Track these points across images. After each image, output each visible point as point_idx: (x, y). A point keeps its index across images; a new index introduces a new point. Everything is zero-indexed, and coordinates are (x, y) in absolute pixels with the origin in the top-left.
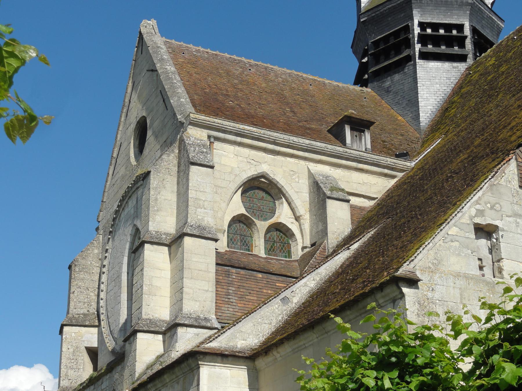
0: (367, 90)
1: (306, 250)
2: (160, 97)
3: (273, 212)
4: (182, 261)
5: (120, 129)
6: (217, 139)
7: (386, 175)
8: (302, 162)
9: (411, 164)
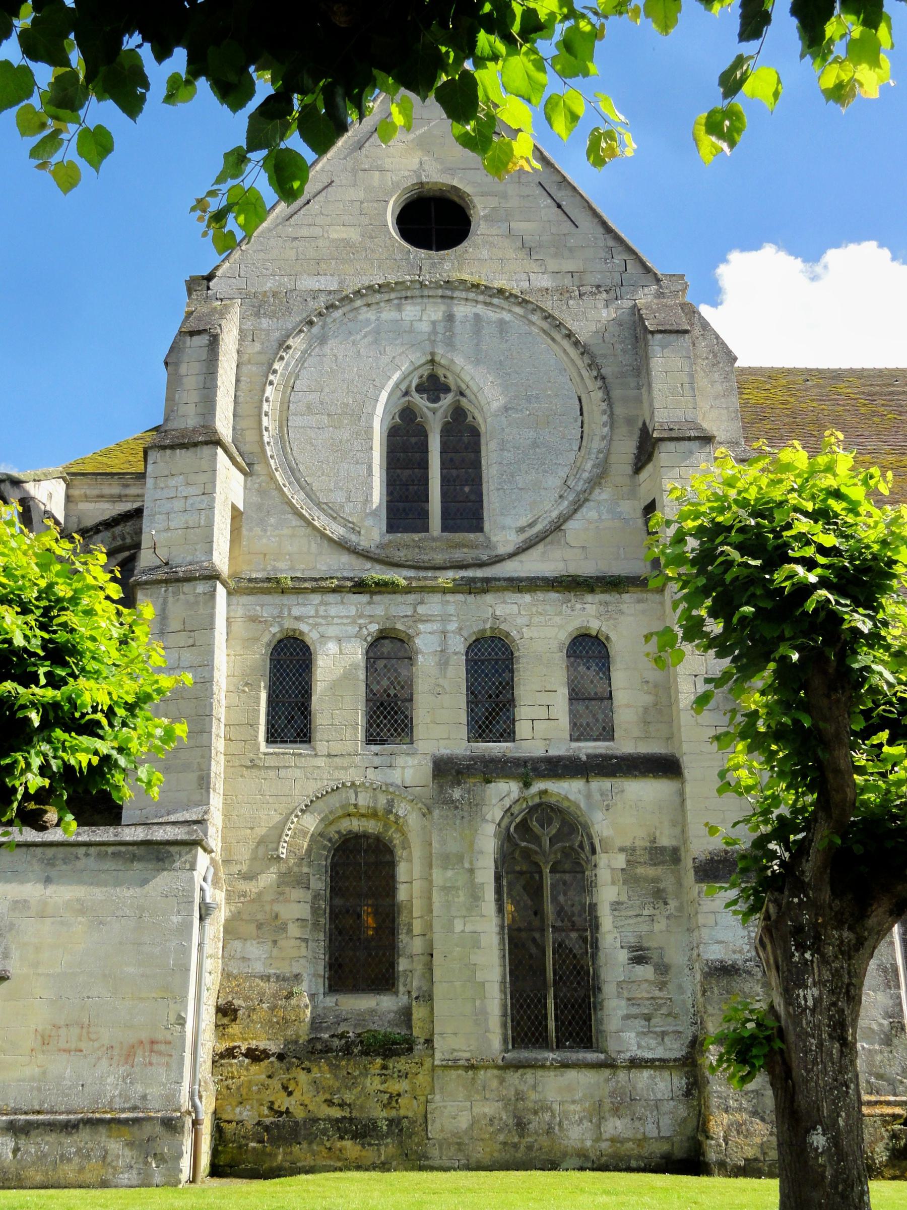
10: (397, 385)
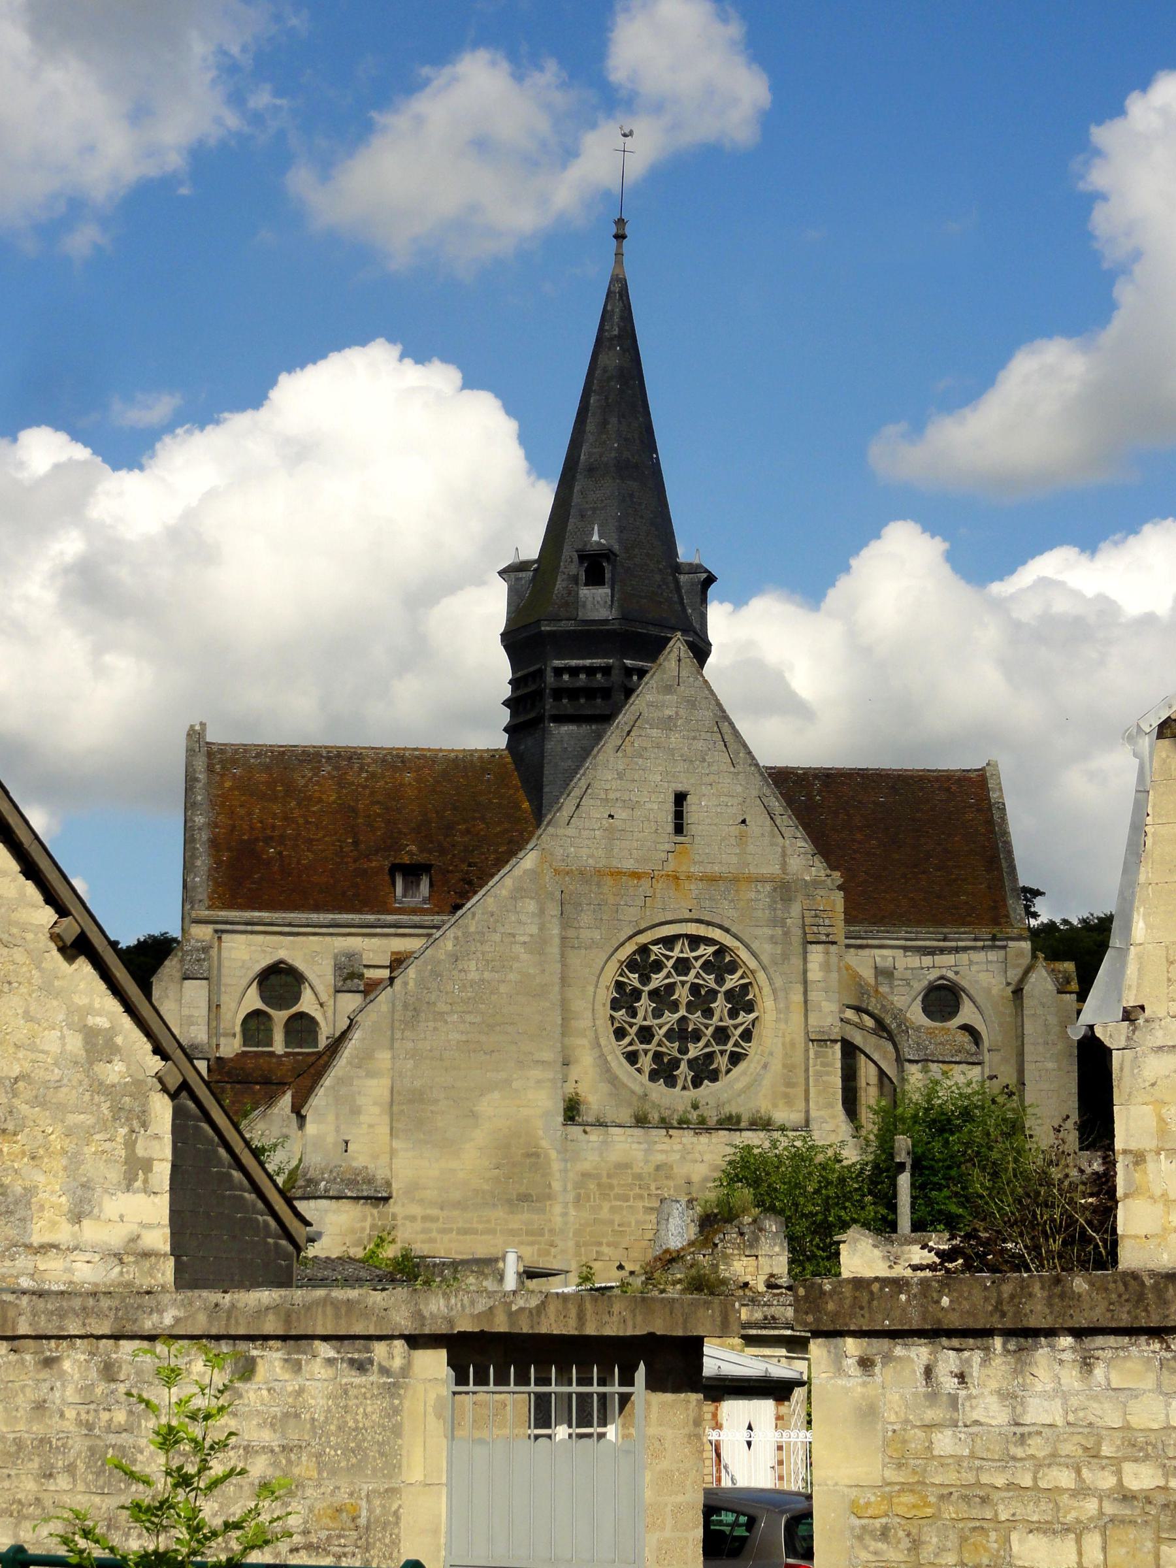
3: (297, 998)
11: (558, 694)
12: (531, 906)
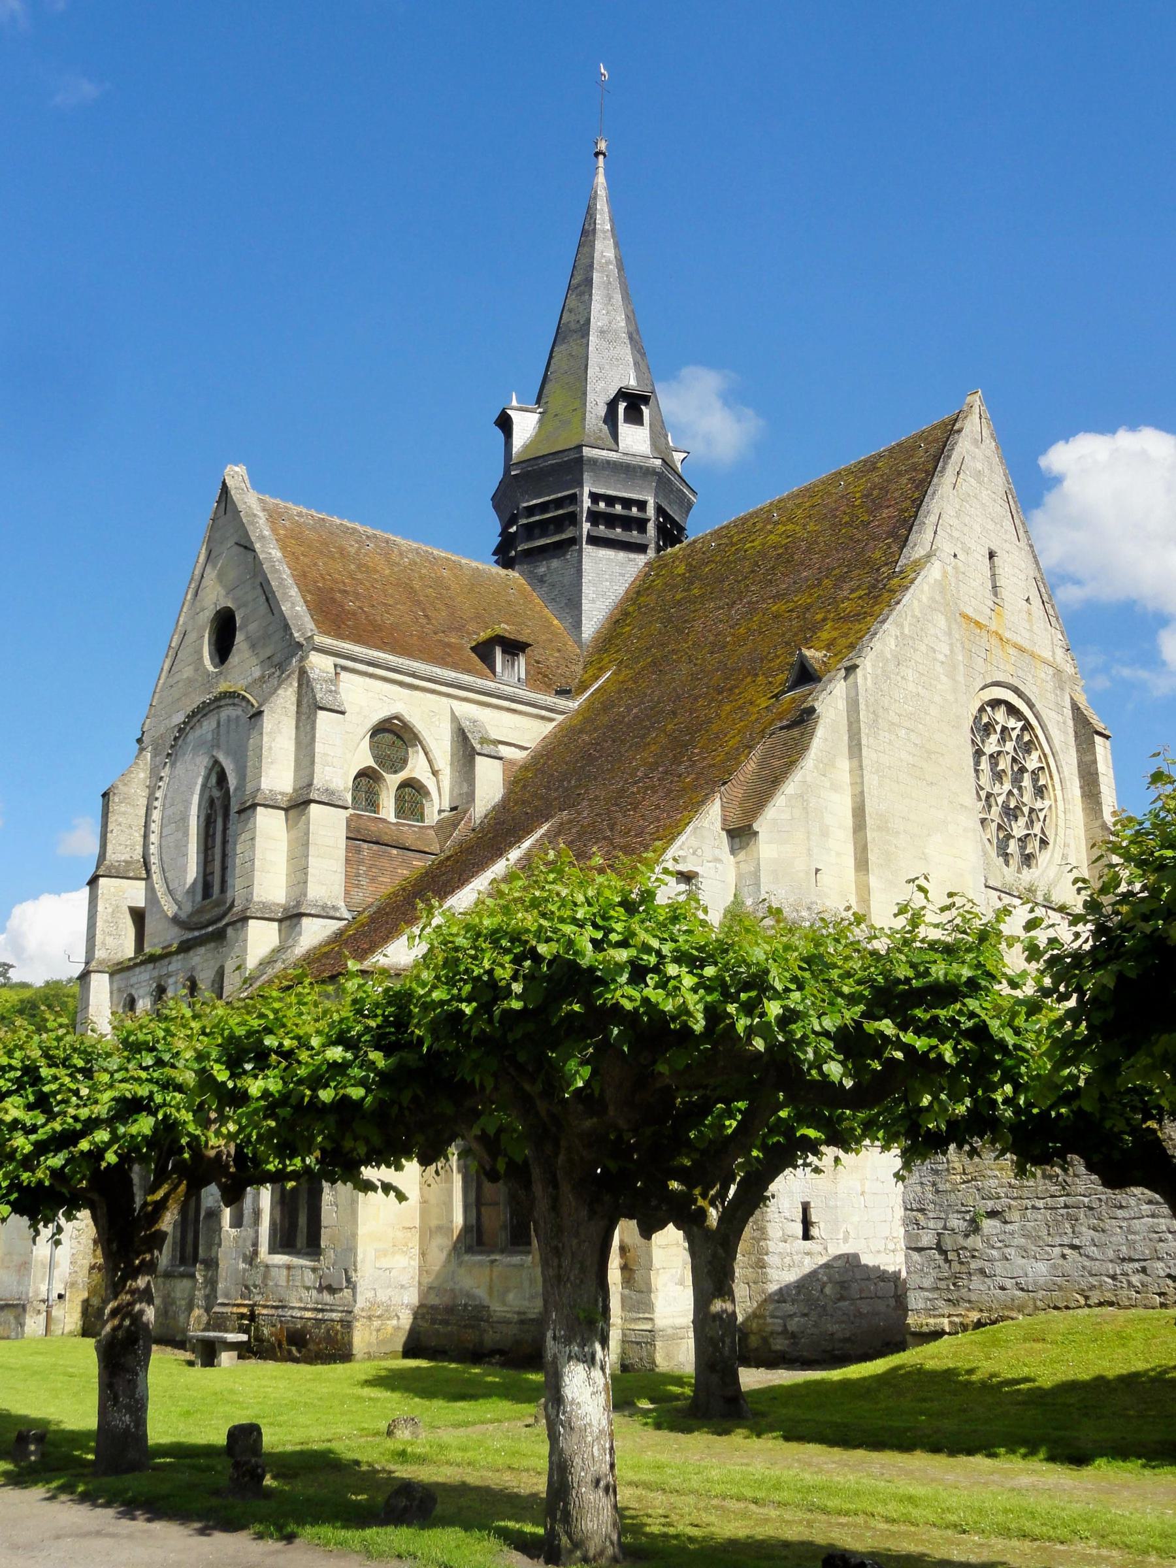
0: (514, 574)
1: (444, 815)
2: (260, 591)
3: (405, 761)
4: (307, 833)
5: (185, 610)
6: (344, 668)
7: (543, 718)
8: (444, 699)
9: (573, 705)
10: (204, 786)
11: (594, 517)
12: (941, 622)
